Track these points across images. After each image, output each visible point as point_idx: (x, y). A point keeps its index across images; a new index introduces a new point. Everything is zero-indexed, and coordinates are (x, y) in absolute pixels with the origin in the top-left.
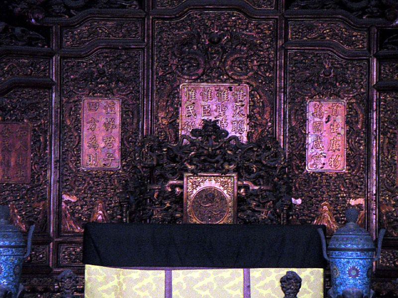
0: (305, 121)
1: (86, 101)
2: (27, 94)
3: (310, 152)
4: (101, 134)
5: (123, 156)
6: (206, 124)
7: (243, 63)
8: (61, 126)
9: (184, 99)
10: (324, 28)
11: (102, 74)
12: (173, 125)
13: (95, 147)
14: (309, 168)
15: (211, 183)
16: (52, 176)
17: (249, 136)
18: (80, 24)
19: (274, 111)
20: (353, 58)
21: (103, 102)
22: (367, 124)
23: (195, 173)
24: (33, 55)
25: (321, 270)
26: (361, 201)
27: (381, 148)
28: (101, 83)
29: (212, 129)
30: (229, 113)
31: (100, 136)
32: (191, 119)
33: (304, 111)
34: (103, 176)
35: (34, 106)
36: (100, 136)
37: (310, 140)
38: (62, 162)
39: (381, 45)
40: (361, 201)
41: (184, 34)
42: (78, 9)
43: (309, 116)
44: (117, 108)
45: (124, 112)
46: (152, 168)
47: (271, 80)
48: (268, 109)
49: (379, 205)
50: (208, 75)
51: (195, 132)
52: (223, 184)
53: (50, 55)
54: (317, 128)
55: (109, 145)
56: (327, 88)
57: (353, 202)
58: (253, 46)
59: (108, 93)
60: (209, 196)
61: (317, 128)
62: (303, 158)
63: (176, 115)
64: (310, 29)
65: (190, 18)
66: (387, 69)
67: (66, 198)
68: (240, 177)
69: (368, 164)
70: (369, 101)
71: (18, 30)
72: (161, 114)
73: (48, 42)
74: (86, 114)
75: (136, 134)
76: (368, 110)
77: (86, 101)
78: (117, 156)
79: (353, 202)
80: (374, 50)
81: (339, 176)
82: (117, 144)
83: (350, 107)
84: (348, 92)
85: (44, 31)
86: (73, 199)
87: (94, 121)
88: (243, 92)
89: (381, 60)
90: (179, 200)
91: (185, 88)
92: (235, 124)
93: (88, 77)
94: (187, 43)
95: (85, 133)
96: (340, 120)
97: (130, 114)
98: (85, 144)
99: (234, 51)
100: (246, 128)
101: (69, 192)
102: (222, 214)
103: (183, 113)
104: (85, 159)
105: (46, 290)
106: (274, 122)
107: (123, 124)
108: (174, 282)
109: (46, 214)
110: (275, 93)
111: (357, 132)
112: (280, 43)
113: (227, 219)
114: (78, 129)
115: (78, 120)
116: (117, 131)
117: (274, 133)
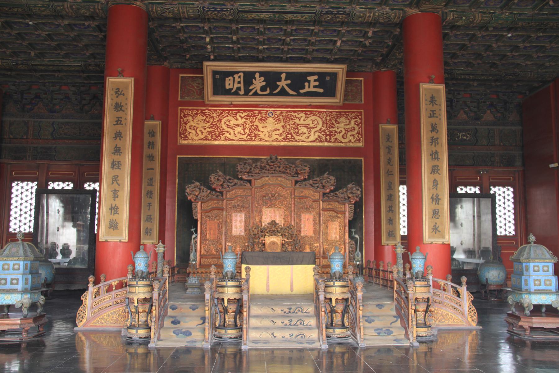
0: (300, 220)
1: (234, 214)
2: (216, 212)
3: (302, 230)
4: (238, 224)
5: (245, 231)
6: (272, 221)
7: (282, 202)
8: (226, 222)
9: (264, 213)
10: (306, 192)
11: (238, 205)
12: (261, 221)
13: (236, 228)
14: (302, 234)
15: (274, 239)
16: (223, 237)
17: (284, 225)
18: (232, 190)
19: (291, 216)
20: (315, 201)
21: (239, 214)
22: (319, 221)
23: (269, 236)
24: (218, 200)
25: (314, 266)
26: (318, 245)
27: (323, 228)
28: (237, 208)
29: (273, 223)
30: (278, 218)
31: (238, 224)
32: (266, 219)
33: (301, 217)
34: (239, 237)
35: (218, 216)
36: (238, 224)
37: (302, 226)
38: (226, 233)
39: (323, 197)
40: (318, 245)
41: (264, 194)
42: (232, 186)
43: (302, 218)
44: (243, 216)
45: (245, 218)
46: (255, 235)
47: (291, 207)
48: (289, 216)
49: (323, 245)
50: (271, 206)
51: (268, 224)
52: (277, 239)
53: (223, 200)
54: (304, 222)
55: (241, 227)
56: (308, 209)
57: (315, 245)
58: (285, 197)
59: (240, 211)
60: (273, 243)
61: (304, 222)
62: (300, 231)
63: (261, 218)
64: (302, 192)
65: (266, 189)
66: (325, 204)
67: (228, 244)
68: (282, 237)
69: (319, 233)
70: (320, 214)
71: (214, 192)
72: (257, 218)
73: (222, 196)
74: (234, 218)
75: (249, 224)
76: (320, 217)
77: (234, 214)
78: (243, 231)
79: (315, 245)
80: (321, 198)
81: (311, 237)
82: (243, 227)
83: (314, 216)
84: (313, 211)
85: (221, 193)
86: (230, 244)
87: (236, 220)
88: (282, 211)
89: (323, 202)
90: (264, 244)
91: (264, 209)
92: (280, 220)
93: (234, 207)
94: (265, 196)
95: (234, 224)
96: (311, 220)
97: (247, 218)
98: (234, 227)
99: (279, 199)
100: (283, 222)
101: (229, 242)
102: (277, 248)
103: (263, 217)
104: (233, 232)
105: (206, 273)
106: (291, 220)
107: (245, 221)
108: (270, 270)
109: (221, 249)
110: (291, 211)
111: (317, 223)
112: (293, 196)
113: (279, 250)
114: (231, 223)
115: (231, 220)
116: (243, 224)
117: (291, 224)
